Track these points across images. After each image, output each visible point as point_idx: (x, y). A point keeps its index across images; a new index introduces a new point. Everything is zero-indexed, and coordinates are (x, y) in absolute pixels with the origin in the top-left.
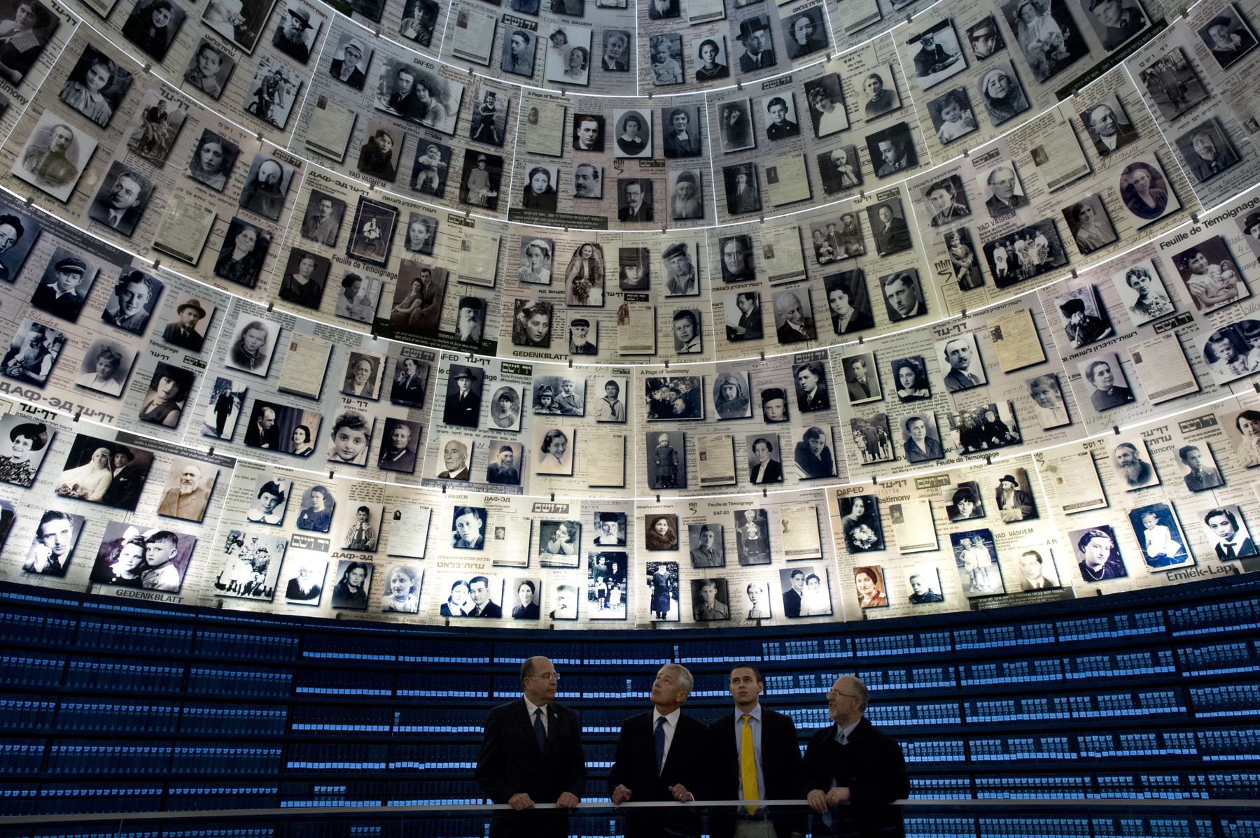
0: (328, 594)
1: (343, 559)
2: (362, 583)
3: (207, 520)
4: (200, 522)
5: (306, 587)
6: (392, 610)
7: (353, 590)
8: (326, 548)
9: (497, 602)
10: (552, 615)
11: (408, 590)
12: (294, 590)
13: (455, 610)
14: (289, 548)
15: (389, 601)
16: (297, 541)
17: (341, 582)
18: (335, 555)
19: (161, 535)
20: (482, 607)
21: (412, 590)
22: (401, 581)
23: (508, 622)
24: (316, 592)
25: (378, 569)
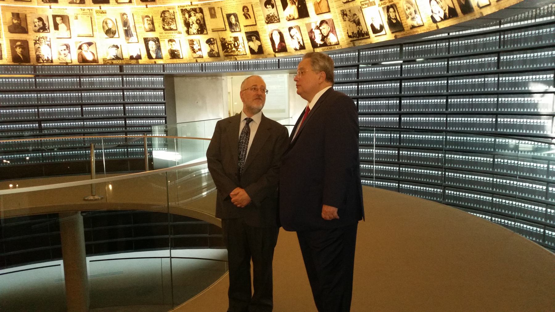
0: (386, 26)
1: (383, 6)
2: (396, 16)
3: (331, 10)
4: (329, 12)
5: (378, 27)
6: (413, 27)
7: (394, 21)
8: (375, 4)
9: (452, 6)
10: (478, 6)
11: (414, 13)
12: (375, 31)
13: (438, 19)
14: (363, 9)
15: (409, 22)
16: (363, 5)
17: (388, 19)
18: (379, 5)
19: (322, 22)
20: (447, 11)
21: (415, 11)
22: (409, 8)
23: (463, 19)
24: (382, 27)
25: (398, 6)
